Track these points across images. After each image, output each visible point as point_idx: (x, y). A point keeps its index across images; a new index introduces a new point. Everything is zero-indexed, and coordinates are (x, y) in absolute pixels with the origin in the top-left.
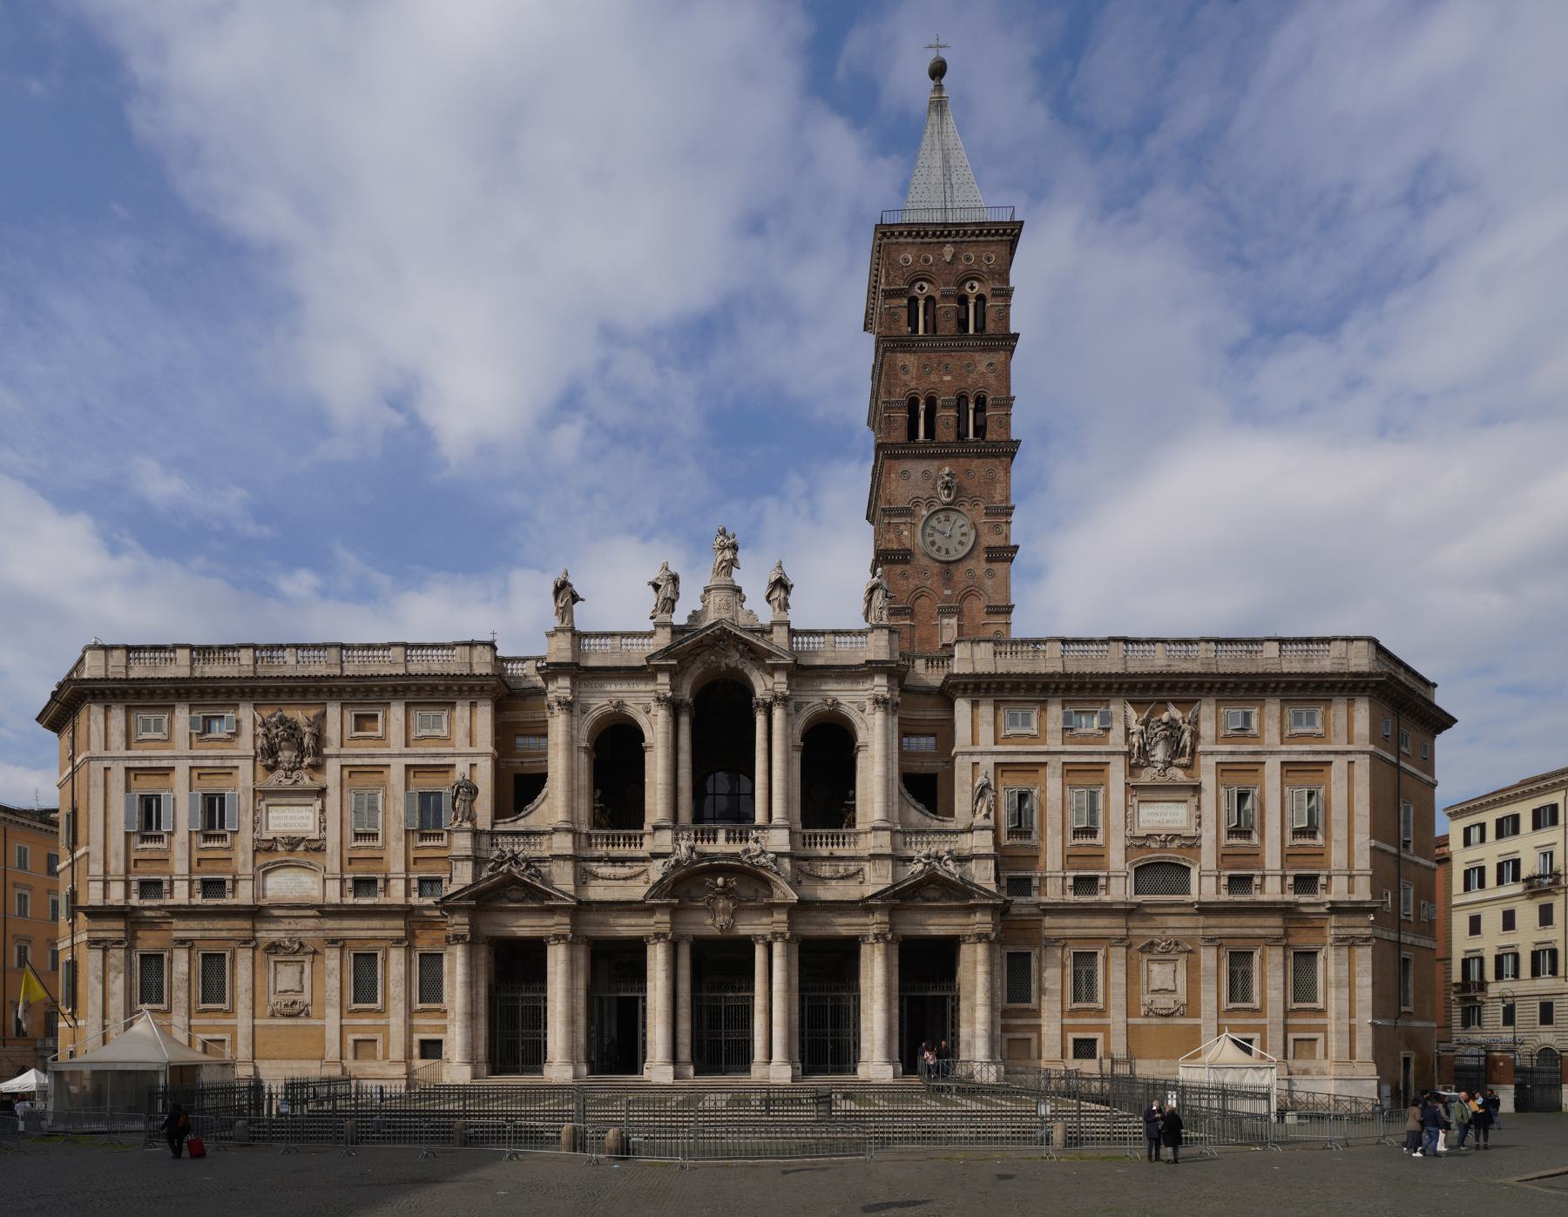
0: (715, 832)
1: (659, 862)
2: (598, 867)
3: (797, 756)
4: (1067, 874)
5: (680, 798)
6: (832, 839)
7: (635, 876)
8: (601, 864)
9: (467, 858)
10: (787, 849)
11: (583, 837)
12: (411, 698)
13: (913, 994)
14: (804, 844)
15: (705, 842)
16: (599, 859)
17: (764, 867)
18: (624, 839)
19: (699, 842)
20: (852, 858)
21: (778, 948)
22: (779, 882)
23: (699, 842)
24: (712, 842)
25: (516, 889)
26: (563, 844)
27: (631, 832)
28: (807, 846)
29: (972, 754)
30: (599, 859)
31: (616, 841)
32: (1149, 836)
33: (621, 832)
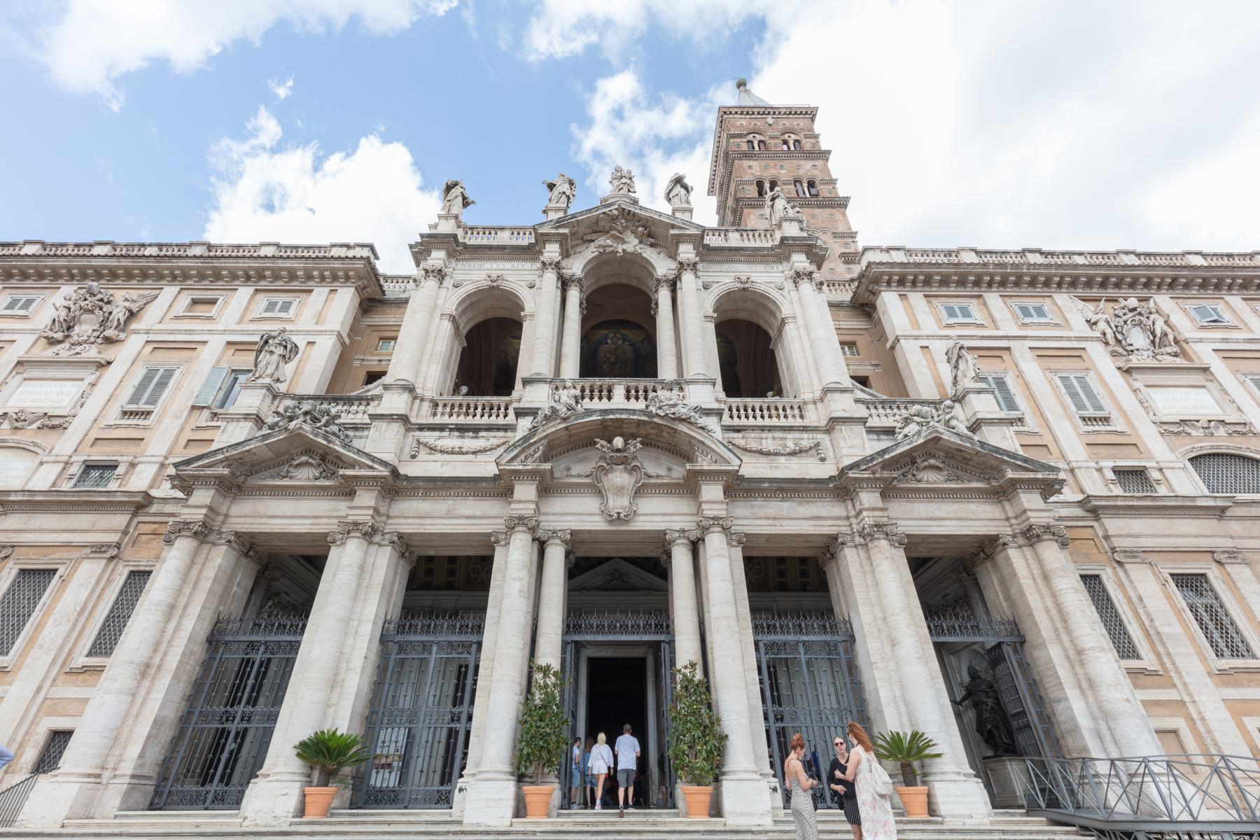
0: (610, 391)
1: (525, 424)
3: (711, 327)
4: (1102, 464)
6: (769, 409)
7: (491, 449)
8: (444, 434)
9: (246, 417)
10: (716, 406)
11: (426, 405)
12: (264, 284)
13: (942, 639)
14: (731, 417)
15: (596, 400)
16: (441, 428)
18: (484, 409)
19: (587, 400)
20: (805, 429)
21: (715, 544)
22: (708, 442)
23: (587, 400)
24: (605, 400)
25: (306, 464)
26: (394, 403)
27: (495, 400)
29: (917, 338)
30: (441, 428)
31: (472, 410)
32: (1182, 421)
33: (480, 398)
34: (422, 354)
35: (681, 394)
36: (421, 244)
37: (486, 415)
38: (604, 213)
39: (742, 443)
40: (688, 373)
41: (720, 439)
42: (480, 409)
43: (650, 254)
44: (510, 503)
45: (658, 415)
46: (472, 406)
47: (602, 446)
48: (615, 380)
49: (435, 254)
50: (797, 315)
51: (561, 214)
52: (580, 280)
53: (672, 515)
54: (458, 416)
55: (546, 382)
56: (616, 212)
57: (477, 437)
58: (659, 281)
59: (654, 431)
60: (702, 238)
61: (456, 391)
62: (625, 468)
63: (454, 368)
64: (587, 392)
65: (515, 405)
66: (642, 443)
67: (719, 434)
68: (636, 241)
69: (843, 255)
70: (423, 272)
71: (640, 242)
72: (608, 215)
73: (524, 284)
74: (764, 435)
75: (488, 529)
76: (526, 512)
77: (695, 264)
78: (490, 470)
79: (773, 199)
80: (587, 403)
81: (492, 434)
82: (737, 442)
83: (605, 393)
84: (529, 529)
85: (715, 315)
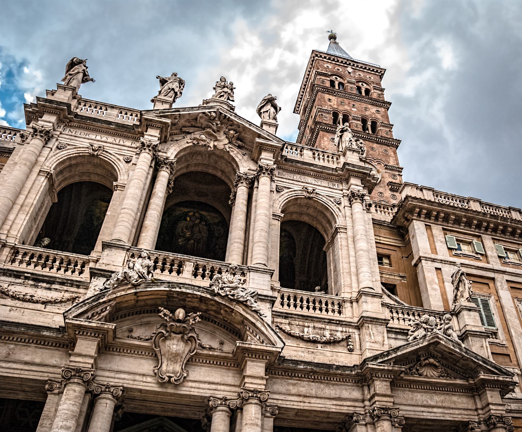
0: (180, 265)
1: (98, 283)
2: (11, 284)
3: (277, 224)
5: (143, 234)
6: (314, 302)
7: (61, 302)
14: (282, 304)
15: (166, 272)
16: (17, 275)
17: (244, 304)
18: (61, 263)
19: (158, 271)
22: (259, 324)
23: (158, 271)
24: (174, 274)
27: (73, 256)
28: (286, 307)
30: (17, 275)
31: (50, 263)
33: (60, 253)
34: (14, 203)
35: (243, 278)
36: (36, 105)
37: (63, 270)
38: (204, 113)
39: (287, 328)
40: (251, 261)
41: (270, 323)
42: (57, 263)
43: (236, 154)
44: (70, 355)
45: (218, 294)
46: (51, 258)
47: (165, 315)
48: (186, 257)
49: (46, 117)
50: (349, 228)
51: (167, 106)
52: (172, 163)
53: (218, 384)
54: (35, 266)
55: (123, 249)
56: (214, 114)
57: (50, 289)
58: (239, 177)
59: (214, 308)
60: (282, 150)
61: (38, 242)
62: (182, 338)
63: (41, 221)
64: (160, 264)
65: (92, 265)
66: (201, 317)
67: (269, 319)
68: (227, 141)
69: (390, 183)
70: (32, 130)
71: (230, 143)
72: (207, 115)
73: (121, 158)
74: (306, 324)
75: (44, 377)
76: (84, 365)
77: (272, 170)
78: (58, 321)
79: (342, 131)
80: (157, 274)
81: (65, 288)
82: (283, 327)
83: (175, 267)
84: (84, 382)
85: (282, 215)
